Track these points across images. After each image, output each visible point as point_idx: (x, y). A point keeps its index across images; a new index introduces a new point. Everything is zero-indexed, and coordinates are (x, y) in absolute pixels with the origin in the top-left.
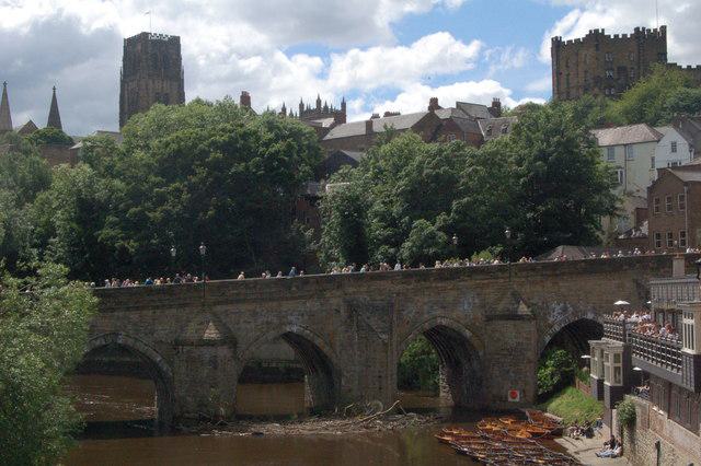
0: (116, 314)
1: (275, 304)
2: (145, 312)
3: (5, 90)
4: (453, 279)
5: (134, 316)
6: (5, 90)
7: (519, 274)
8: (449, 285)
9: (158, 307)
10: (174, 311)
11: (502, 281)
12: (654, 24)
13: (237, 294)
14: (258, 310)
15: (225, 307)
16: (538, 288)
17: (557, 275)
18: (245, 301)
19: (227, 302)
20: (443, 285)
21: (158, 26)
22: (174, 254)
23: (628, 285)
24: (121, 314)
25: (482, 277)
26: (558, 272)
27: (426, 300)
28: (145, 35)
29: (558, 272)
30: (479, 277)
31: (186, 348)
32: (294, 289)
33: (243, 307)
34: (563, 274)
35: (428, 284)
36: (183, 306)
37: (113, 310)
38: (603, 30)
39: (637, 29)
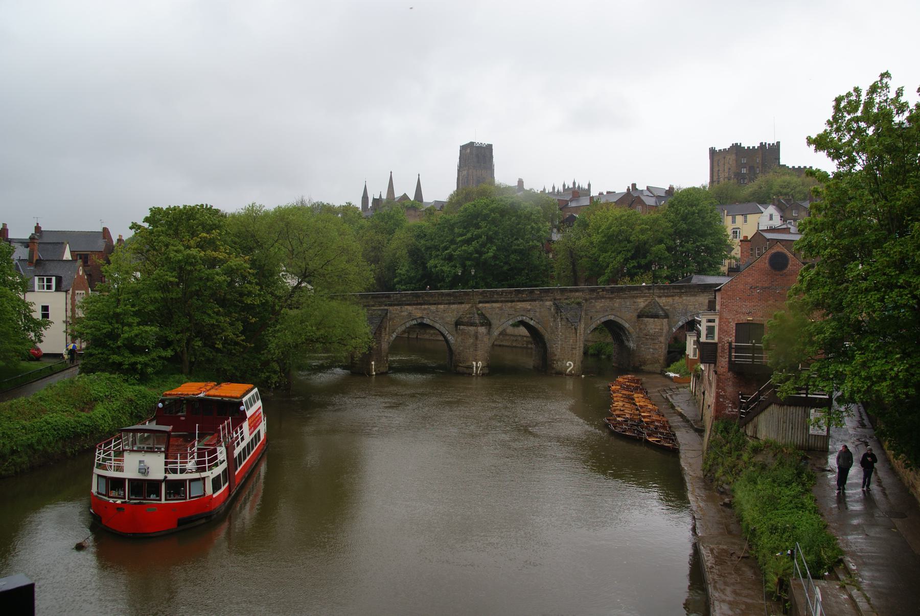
2: (439, 306)
3: (391, 176)
6: (391, 176)
12: (770, 140)
16: (670, 300)
21: (481, 139)
22: (473, 273)
24: (426, 307)
25: (636, 292)
26: (683, 291)
28: (472, 144)
29: (683, 291)
31: (462, 327)
38: (740, 144)
39: (761, 144)
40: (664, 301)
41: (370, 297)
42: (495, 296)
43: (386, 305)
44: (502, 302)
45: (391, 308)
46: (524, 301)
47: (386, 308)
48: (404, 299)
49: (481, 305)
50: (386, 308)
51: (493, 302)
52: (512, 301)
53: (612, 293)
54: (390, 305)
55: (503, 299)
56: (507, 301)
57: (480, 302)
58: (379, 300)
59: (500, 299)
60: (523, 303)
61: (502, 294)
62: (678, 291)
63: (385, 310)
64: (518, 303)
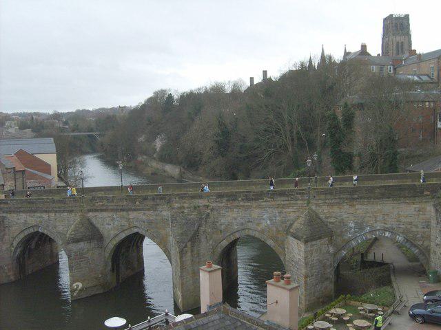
0: (36, 214)
1: (125, 213)
2: (50, 214)
4: (258, 200)
7: (317, 197)
8: (254, 204)
9: (56, 212)
11: (301, 202)
14: (115, 216)
16: (336, 209)
17: (354, 199)
19: (96, 211)
20: (249, 204)
23: (428, 208)
24: (38, 214)
25: (282, 198)
26: (356, 196)
27: (235, 215)
29: (356, 196)
30: (279, 199)
32: (137, 203)
33: (105, 214)
34: (361, 198)
35: (236, 203)
36: (71, 211)
40: (325, 211)
43: (4, 212)
45: (8, 215)
46: (135, 210)
47: (4, 215)
50: (4, 215)
52: (123, 210)
53: (248, 199)
57: (90, 211)
61: (113, 201)
62: (349, 197)
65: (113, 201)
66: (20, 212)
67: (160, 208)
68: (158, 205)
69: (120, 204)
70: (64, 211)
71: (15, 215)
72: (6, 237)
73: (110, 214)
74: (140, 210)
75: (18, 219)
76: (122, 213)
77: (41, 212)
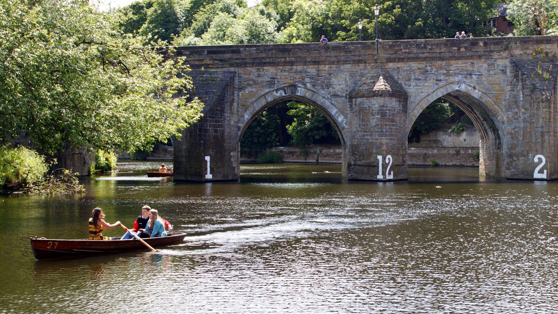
0: (295, 67)
1: (444, 63)
2: (322, 67)
5: (312, 70)
9: (333, 63)
10: (348, 66)
13: (409, 53)
15: (399, 65)
18: (416, 59)
19: (401, 60)
24: (300, 68)
31: (359, 100)
33: (414, 65)
36: (359, 62)
37: (292, 63)
41: (206, 53)
42: (415, 51)
43: (232, 65)
44: (425, 59)
45: (240, 70)
48: (264, 55)
49: (391, 65)
50: (232, 69)
51: (410, 59)
54: (238, 65)
55: (426, 55)
56: (433, 59)
57: (390, 60)
58: (220, 56)
59: (421, 55)
60: (460, 62)
61: (425, 47)
63: (231, 72)
64: (453, 62)
65: (425, 47)
66: (265, 64)
67: (495, 55)
68: (492, 51)
69: (438, 51)
70: (345, 62)
71: (254, 70)
72: (235, 104)
73: (422, 65)
74: (468, 58)
75: (259, 76)
76: (440, 62)
77: (305, 63)
